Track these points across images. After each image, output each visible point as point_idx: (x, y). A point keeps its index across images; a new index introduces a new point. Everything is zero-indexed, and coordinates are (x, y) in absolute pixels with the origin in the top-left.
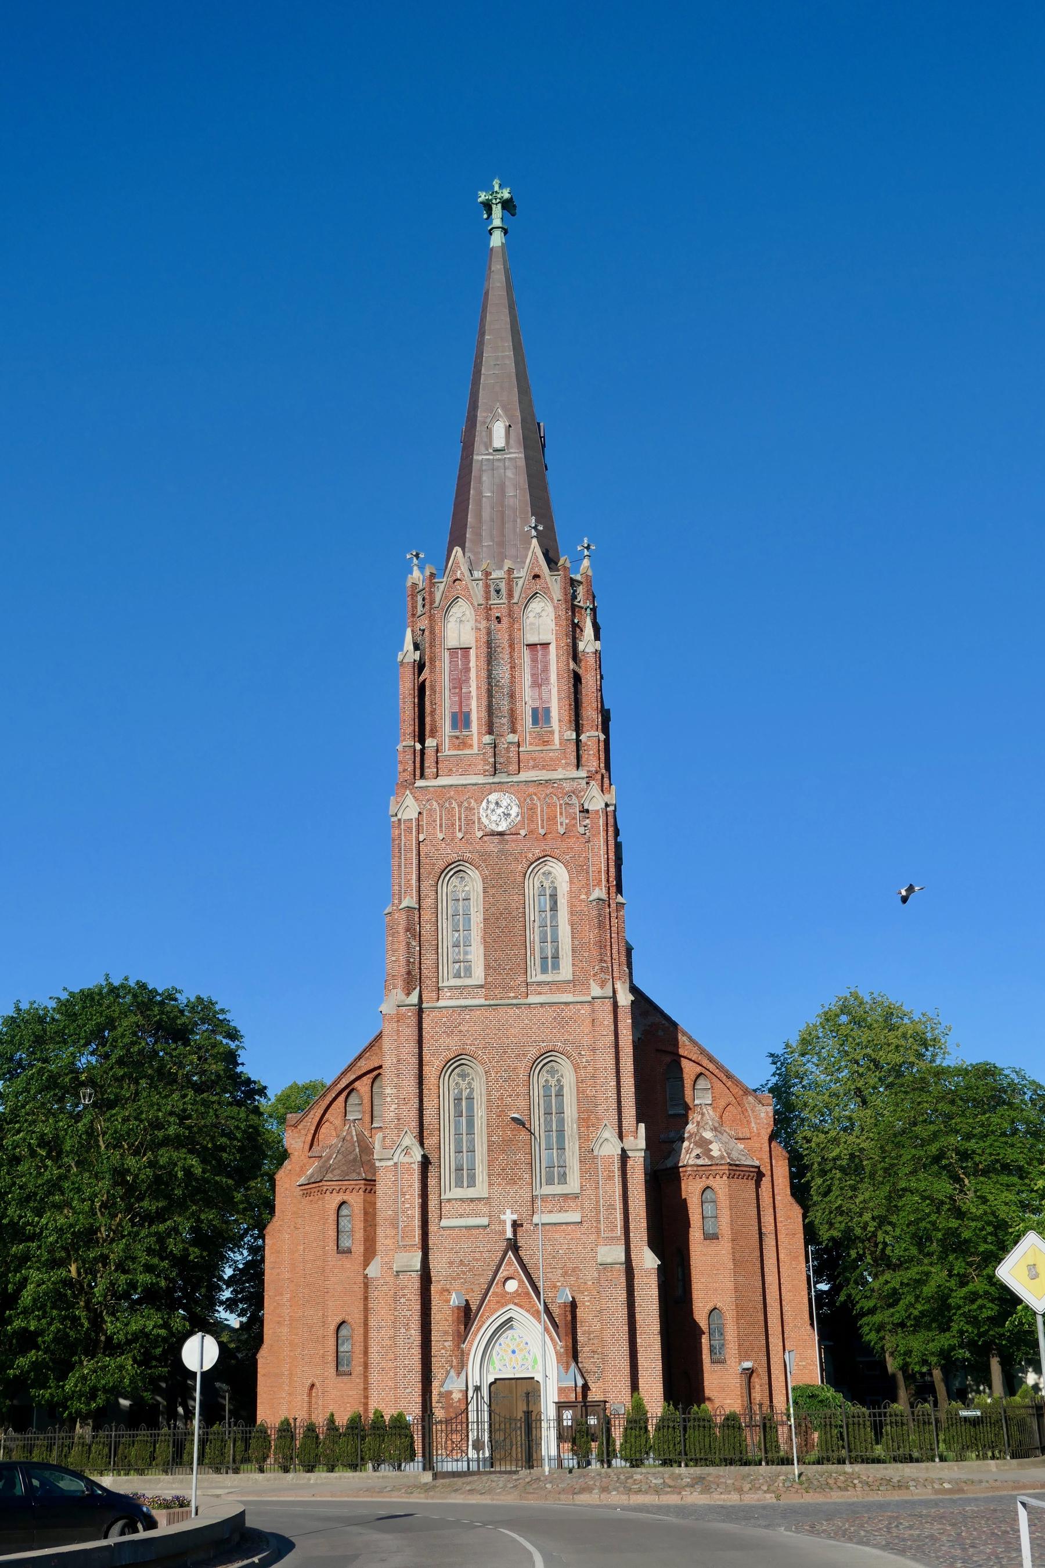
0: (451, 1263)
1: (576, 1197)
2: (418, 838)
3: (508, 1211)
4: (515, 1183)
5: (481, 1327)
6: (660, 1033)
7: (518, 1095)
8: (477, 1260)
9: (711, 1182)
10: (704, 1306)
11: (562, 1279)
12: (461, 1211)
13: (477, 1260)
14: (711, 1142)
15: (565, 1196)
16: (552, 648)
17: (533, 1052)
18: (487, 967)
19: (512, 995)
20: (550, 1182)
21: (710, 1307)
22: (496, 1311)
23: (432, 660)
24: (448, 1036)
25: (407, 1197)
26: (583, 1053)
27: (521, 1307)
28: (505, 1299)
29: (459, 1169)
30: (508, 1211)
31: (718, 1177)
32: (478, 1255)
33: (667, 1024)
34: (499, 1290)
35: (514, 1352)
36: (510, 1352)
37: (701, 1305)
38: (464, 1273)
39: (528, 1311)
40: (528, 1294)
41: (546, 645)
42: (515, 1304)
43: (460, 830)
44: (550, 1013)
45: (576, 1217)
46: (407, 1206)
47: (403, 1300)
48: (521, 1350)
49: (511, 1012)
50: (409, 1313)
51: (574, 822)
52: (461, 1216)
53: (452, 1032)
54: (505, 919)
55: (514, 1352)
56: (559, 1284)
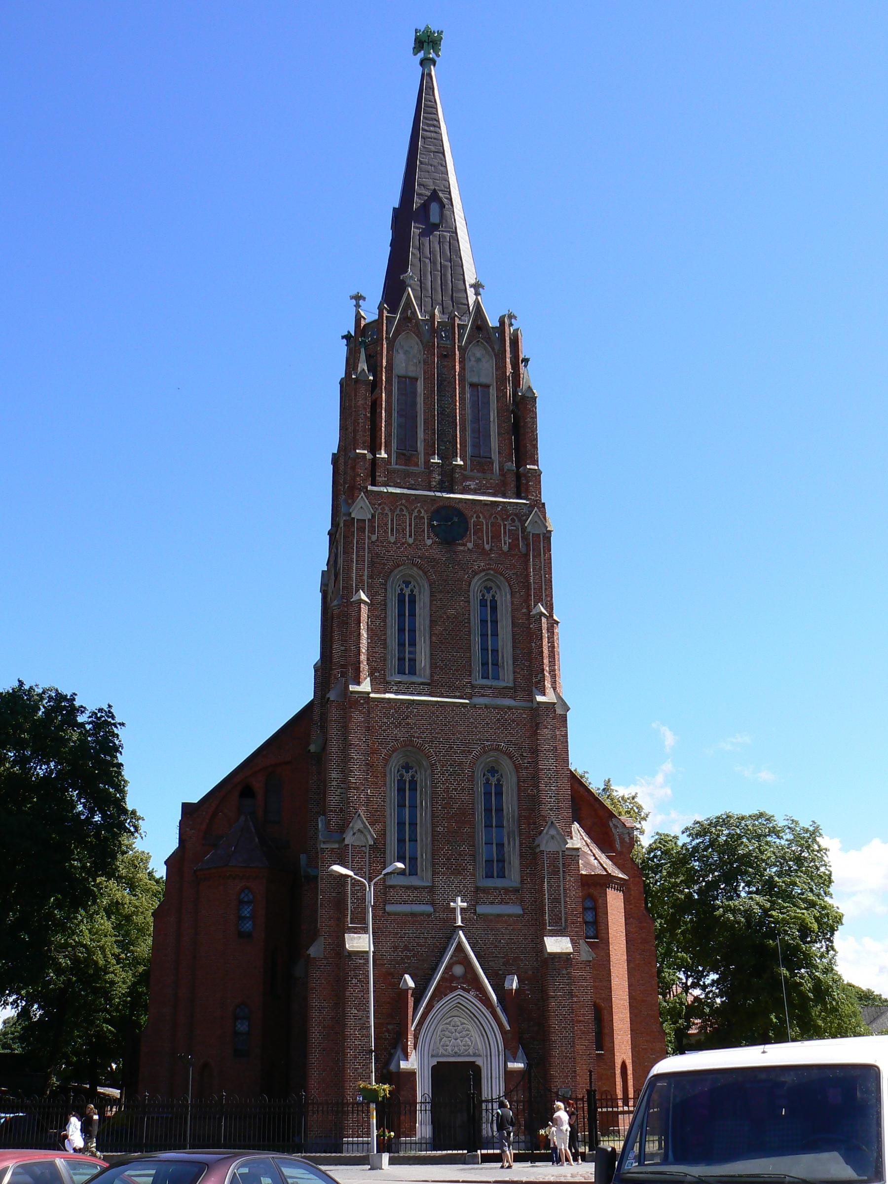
0: (395, 948)
4: (460, 873)
11: (503, 968)
15: (507, 890)
18: (433, 666)
20: (489, 875)
26: (525, 754)
38: (408, 958)
41: (487, 386)
43: (410, 536)
46: (358, 888)
52: (405, 902)
53: (400, 724)
56: (501, 972)
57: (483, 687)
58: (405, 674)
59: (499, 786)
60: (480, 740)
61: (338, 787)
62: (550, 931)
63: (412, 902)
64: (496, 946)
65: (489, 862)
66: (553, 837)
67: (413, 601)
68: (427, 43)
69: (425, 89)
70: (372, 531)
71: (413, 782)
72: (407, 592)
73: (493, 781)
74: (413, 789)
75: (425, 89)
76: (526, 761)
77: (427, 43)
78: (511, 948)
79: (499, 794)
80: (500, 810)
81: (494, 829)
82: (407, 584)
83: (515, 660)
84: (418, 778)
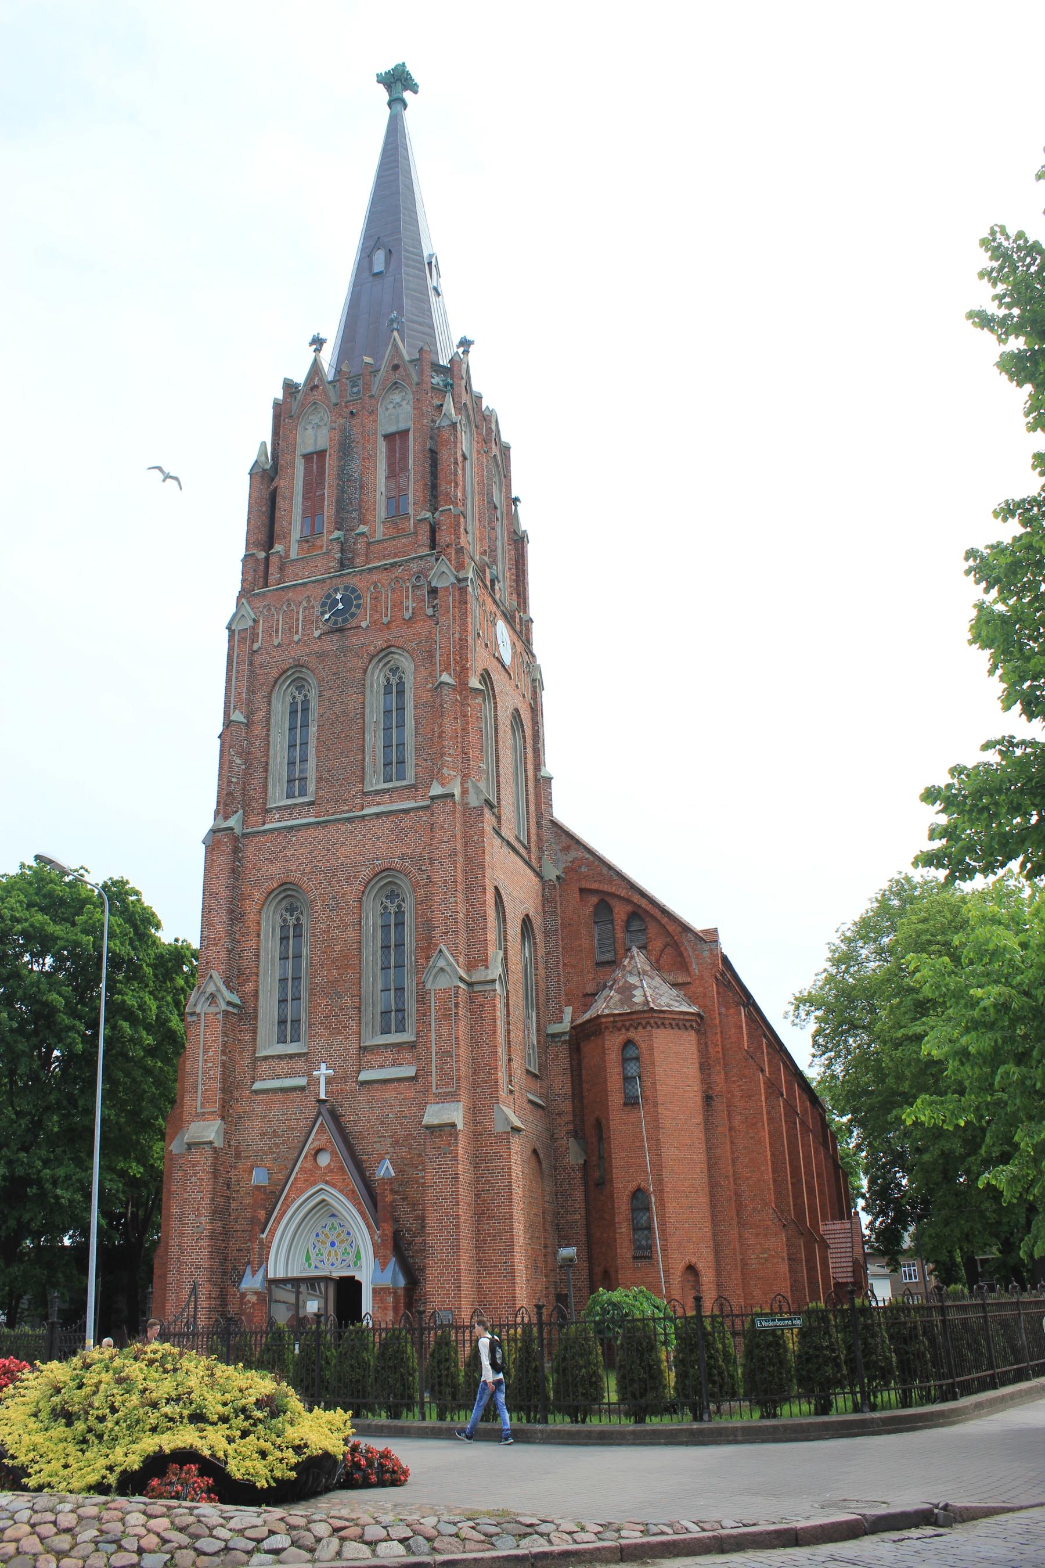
0: (263, 1134)
1: (412, 1045)
2: (251, 646)
3: (323, 1066)
4: (340, 1033)
5: (285, 1212)
6: (584, 869)
7: (347, 926)
8: (293, 1129)
9: (632, 1034)
10: (625, 1188)
11: (391, 1150)
12: (279, 1071)
13: (293, 1129)
14: (636, 987)
15: (399, 1046)
17: (366, 873)
19: (346, 808)
20: (386, 1031)
21: (632, 1186)
22: (302, 1191)
24: (272, 863)
25: (210, 1054)
26: (424, 868)
27: (333, 1186)
28: (312, 1176)
29: (282, 1022)
30: (323, 1066)
31: (640, 1028)
32: (293, 1124)
33: (591, 858)
34: (308, 1165)
35: (333, 1244)
36: (328, 1244)
37: (621, 1186)
39: (341, 1191)
40: (341, 1168)
42: (327, 1183)
44: (388, 823)
45: (409, 1071)
46: (210, 1065)
47: (194, 1179)
48: (342, 1242)
49: (343, 828)
50: (199, 1196)
51: (421, 605)
54: (342, 723)
55: (333, 1244)
58: (294, 797)
59: (400, 913)
60: (369, 860)
62: (437, 1095)
63: (287, 1076)
64: (383, 1123)
65: (385, 1013)
66: (442, 969)
68: (397, 82)
71: (298, 926)
73: (392, 909)
74: (298, 936)
76: (425, 877)
77: (397, 82)
78: (401, 1124)
79: (400, 924)
80: (400, 945)
81: (392, 970)
82: (299, 689)
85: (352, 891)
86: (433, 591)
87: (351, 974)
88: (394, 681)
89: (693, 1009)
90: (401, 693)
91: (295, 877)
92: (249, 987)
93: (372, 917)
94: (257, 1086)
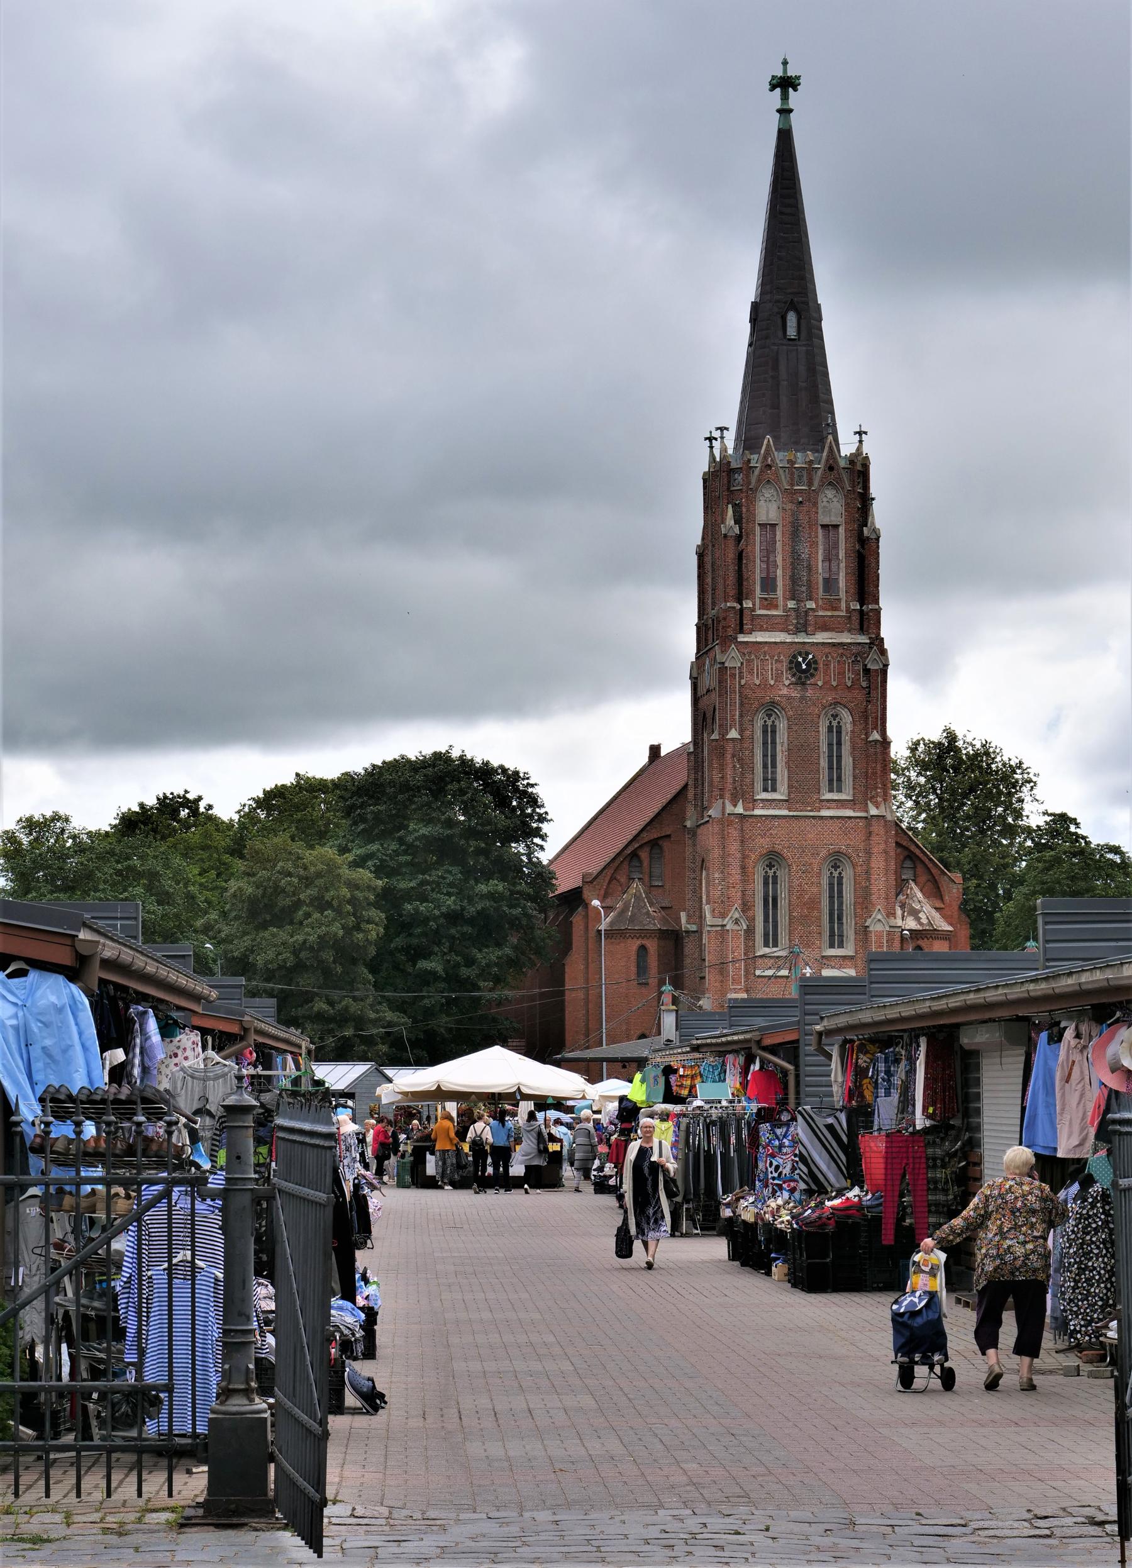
1: (852, 958)
15: (844, 957)
16: (842, 530)
17: (823, 853)
18: (790, 787)
20: (832, 946)
23: (747, 534)
41: (836, 527)
57: (828, 801)
59: (840, 878)
61: (720, 883)
67: (774, 732)
69: (785, 138)
70: (741, 678)
71: (775, 877)
72: (769, 723)
73: (836, 874)
74: (775, 882)
75: (785, 138)
77: (785, 84)
82: (769, 716)
83: (855, 777)
84: (778, 873)
85: (816, 862)
86: (867, 671)
87: (815, 913)
88: (835, 724)
89: (950, 928)
90: (839, 732)
91: (778, 848)
92: (750, 913)
93: (825, 882)
94: (758, 973)
